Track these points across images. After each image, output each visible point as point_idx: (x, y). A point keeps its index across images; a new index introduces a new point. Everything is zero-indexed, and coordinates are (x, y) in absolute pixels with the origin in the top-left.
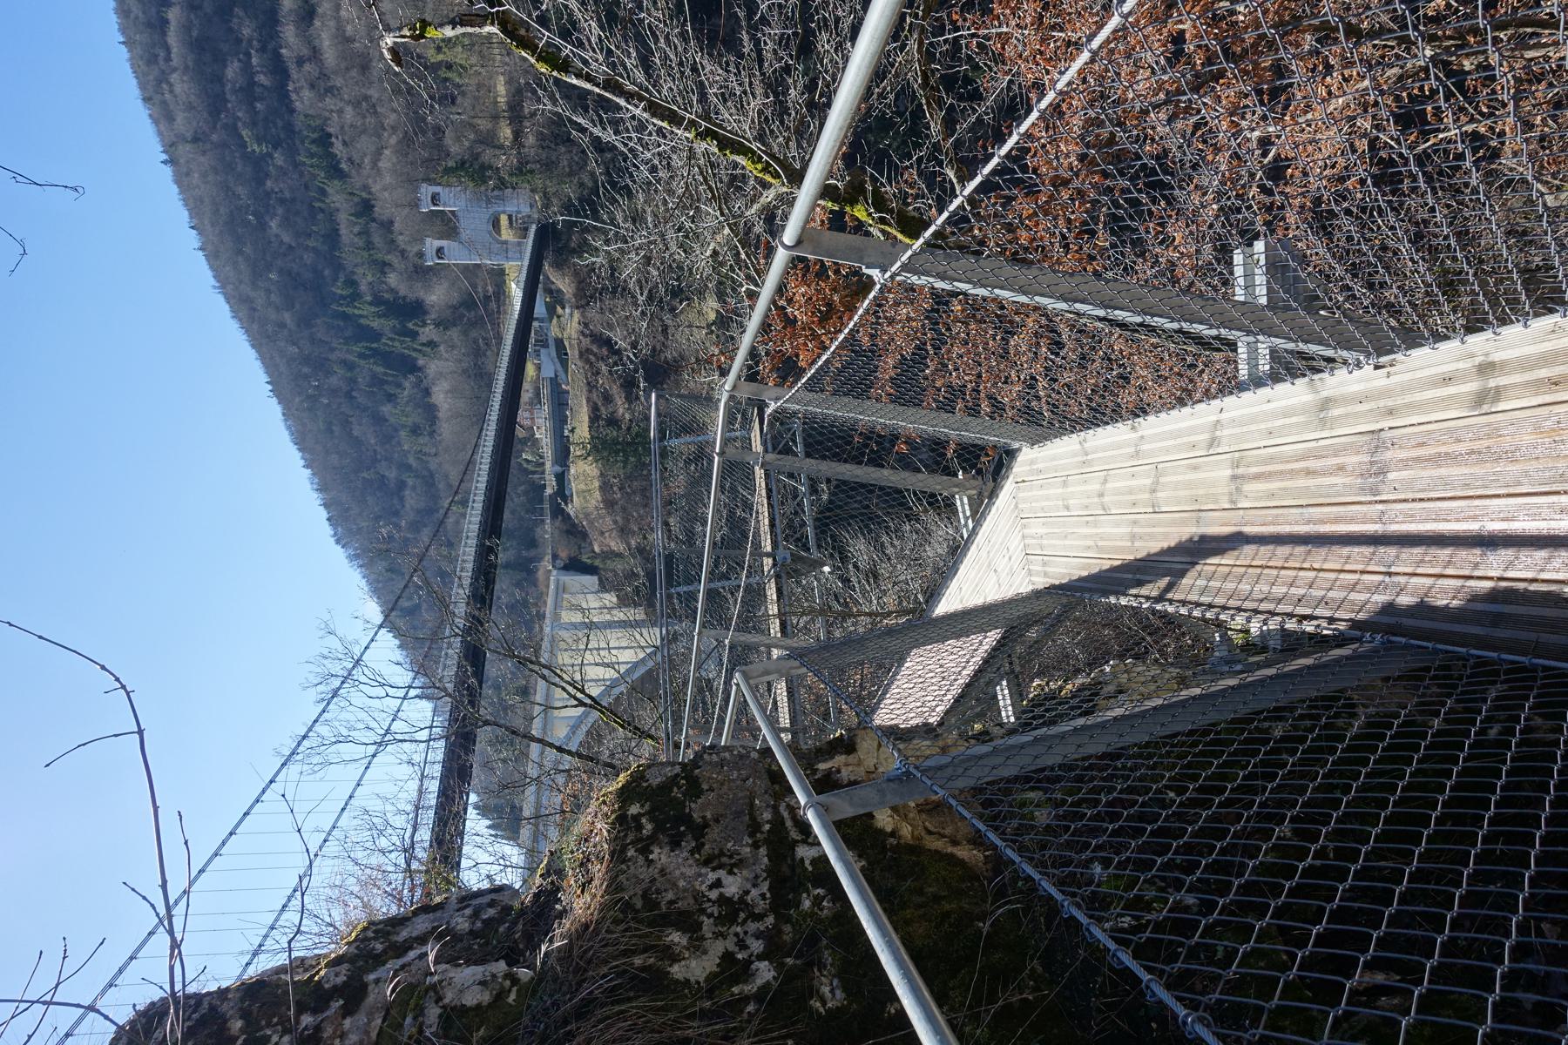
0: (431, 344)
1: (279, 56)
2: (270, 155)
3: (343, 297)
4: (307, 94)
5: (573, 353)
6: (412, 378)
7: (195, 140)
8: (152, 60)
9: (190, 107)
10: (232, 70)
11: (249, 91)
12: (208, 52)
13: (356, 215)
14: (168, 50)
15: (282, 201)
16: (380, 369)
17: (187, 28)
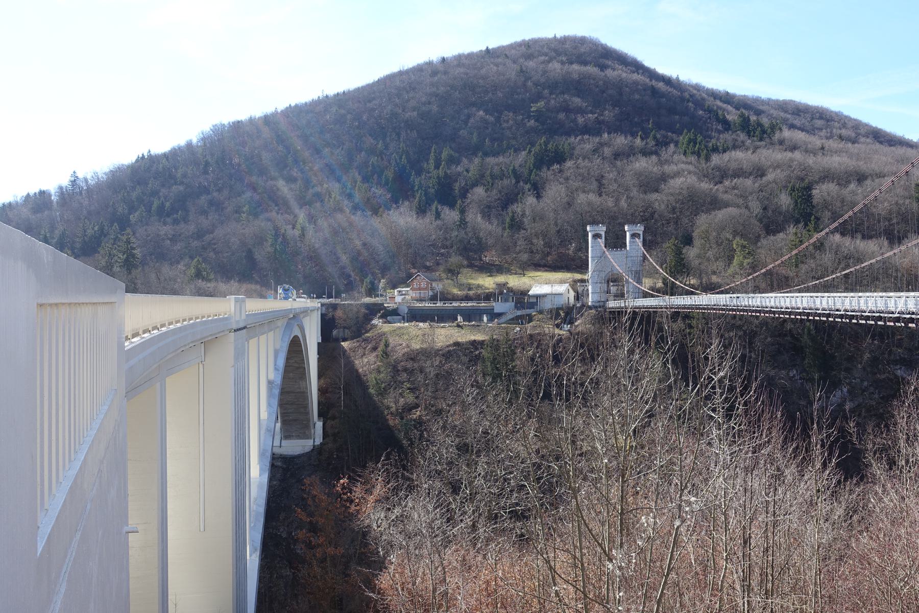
0: (438, 215)
1: (598, 133)
2: (529, 117)
3: (441, 153)
4: (588, 147)
5: (529, 328)
6: (389, 196)
7: (522, 71)
8: (558, 53)
9: (545, 72)
10: (577, 101)
11: (567, 109)
12: (578, 86)
13: (514, 168)
14: (571, 63)
15: (498, 119)
16: (390, 174)
17: (590, 76)
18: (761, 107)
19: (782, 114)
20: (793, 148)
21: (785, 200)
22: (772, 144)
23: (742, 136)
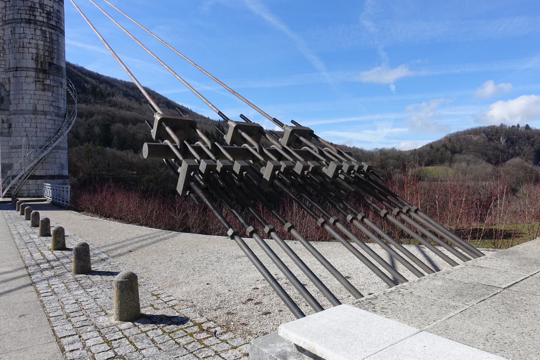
18: (115, 84)
19: (125, 89)
20: (115, 105)
21: (97, 130)
22: (105, 102)
23: (90, 97)
